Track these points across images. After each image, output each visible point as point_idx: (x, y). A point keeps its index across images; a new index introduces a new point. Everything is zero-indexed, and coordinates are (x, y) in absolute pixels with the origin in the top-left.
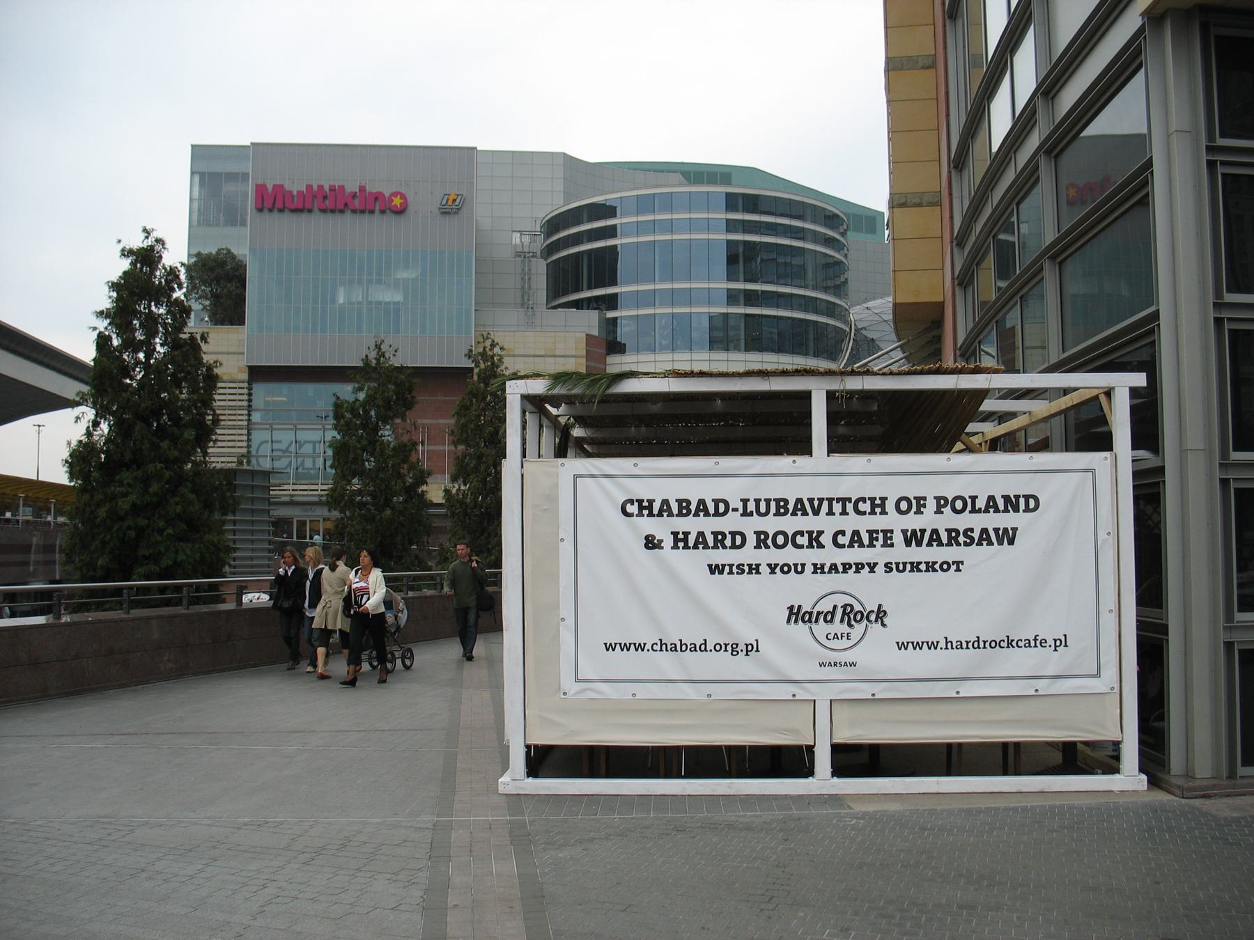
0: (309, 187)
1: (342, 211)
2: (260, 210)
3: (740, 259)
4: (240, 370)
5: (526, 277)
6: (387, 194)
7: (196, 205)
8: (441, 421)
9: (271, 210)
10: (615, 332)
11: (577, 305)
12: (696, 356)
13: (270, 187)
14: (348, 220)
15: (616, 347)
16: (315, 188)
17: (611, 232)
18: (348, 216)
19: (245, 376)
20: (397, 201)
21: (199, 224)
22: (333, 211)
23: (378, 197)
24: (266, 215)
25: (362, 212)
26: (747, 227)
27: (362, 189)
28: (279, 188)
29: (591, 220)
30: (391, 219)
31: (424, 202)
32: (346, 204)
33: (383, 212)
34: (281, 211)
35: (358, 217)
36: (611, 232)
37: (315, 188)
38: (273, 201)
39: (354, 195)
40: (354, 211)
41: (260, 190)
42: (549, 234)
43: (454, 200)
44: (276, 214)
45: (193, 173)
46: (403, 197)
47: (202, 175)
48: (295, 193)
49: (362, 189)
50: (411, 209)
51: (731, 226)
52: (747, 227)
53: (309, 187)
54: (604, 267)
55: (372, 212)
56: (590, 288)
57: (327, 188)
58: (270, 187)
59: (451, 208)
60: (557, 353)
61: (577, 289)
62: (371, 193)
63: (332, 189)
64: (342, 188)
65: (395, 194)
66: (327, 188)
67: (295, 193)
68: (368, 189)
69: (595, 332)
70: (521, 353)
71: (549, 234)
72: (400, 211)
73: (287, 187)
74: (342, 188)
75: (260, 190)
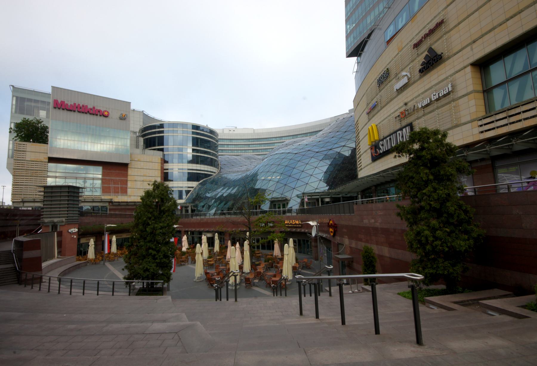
0: (75, 104)
1: (86, 113)
2: (55, 108)
3: (196, 142)
4: (45, 158)
7: (14, 107)
8: (117, 178)
9: (59, 109)
11: (154, 149)
12: (184, 165)
13: (59, 101)
14: (88, 116)
16: (77, 104)
17: (162, 132)
18: (88, 115)
19: (47, 161)
20: (106, 113)
21: (16, 112)
22: (83, 113)
23: (99, 111)
24: (57, 110)
25: (94, 114)
26: (198, 134)
27: (94, 108)
28: (63, 102)
30: (102, 118)
31: (115, 115)
33: (100, 116)
34: (63, 109)
35: (92, 116)
36: (162, 132)
37: (77, 104)
38: (59, 106)
39: (91, 109)
40: (91, 114)
41: (56, 102)
42: (142, 132)
44: (61, 111)
45: (13, 96)
46: (108, 112)
47: (17, 98)
48: (69, 105)
49: (94, 108)
50: (110, 116)
51: (193, 133)
52: (198, 134)
53: (75, 104)
54: (161, 141)
55: (97, 115)
56: (158, 145)
57: (81, 105)
58: (59, 101)
59: (123, 118)
61: (154, 146)
63: (83, 106)
64: (87, 106)
65: (106, 111)
66: (81, 105)
67: (69, 105)
71: (142, 132)
72: (106, 116)
73: (66, 102)
74: (87, 106)
75: (56, 102)
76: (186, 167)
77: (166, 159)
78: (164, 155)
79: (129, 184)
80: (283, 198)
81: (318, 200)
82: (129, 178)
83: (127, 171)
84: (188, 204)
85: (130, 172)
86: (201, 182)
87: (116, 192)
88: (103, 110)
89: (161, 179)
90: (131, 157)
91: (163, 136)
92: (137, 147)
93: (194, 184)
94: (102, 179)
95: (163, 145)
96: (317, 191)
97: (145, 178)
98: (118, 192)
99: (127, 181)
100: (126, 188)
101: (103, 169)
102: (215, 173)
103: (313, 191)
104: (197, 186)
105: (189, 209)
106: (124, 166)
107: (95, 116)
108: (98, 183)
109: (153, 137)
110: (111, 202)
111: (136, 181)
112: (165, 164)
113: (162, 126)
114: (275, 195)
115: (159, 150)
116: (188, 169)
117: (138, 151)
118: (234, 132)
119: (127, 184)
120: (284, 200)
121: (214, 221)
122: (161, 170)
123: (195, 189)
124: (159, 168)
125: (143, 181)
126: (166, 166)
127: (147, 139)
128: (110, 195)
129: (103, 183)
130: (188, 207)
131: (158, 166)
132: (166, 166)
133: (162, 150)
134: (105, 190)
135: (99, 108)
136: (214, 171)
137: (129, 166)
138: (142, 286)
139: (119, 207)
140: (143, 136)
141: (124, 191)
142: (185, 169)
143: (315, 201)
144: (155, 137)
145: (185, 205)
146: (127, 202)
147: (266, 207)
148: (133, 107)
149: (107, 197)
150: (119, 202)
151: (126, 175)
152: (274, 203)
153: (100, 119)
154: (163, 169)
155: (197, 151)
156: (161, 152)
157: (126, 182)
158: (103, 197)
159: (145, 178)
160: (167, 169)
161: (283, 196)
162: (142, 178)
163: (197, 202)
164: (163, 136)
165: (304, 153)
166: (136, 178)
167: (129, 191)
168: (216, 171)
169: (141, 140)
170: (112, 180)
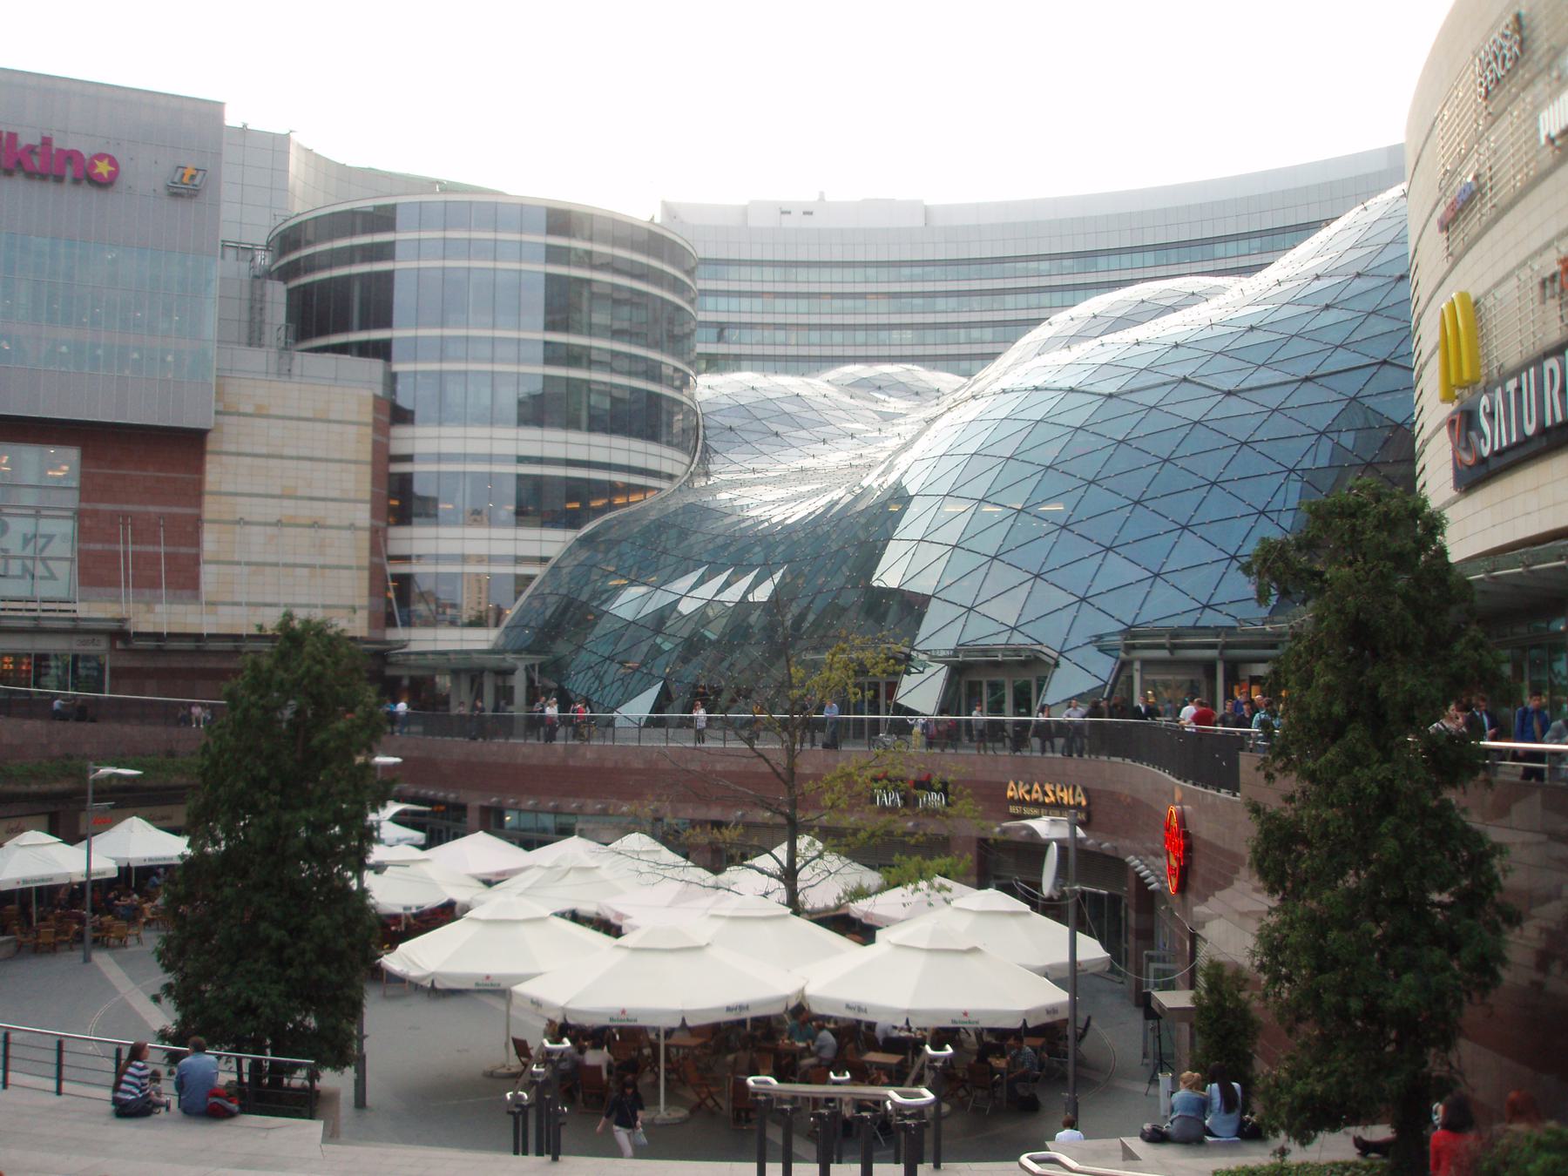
5: (256, 307)
6: (87, 157)
8: (151, 509)
10: (394, 391)
15: (402, 416)
17: (384, 252)
20: (103, 168)
23: (72, 156)
25: (44, 177)
27: (47, 142)
29: (365, 231)
30: (84, 196)
31: (145, 171)
32: (19, 163)
33: (77, 181)
36: (384, 252)
39: (31, 149)
40: (31, 175)
43: (193, 177)
46: (113, 162)
49: (47, 142)
54: (376, 302)
55: (59, 179)
56: (364, 326)
59: (187, 189)
60: (333, 416)
61: (345, 327)
62: (60, 151)
65: (101, 157)
68: (56, 144)
69: (380, 391)
70: (280, 412)
76: (510, 449)
77: (404, 401)
78: (392, 379)
79: (210, 541)
80: (1017, 651)
81: (1209, 668)
82: (210, 508)
83: (199, 469)
84: (510, 659)
85: (216, 473)
86: (587, 528)
87: (146, 580)
88: (87, 151)
89: (375, 514)
90: (220, 395)
91: (389, 276)
92: (254, 338)
93: (553, 542)
94: (80, 515)
95: (387, 323)
96: (1210, 619)
97: (289, 508)
98: (154, 584)
99: (197, 522)
100: (196, 560)
101: (84, 457)
102: (671, 477)
103: (1187, 621)
104: (570, 551)
105: (519, 682)
106: (182, 447)
107: (51, 187)
108: (62, 531)
109: (334, 287)
110: (119, 634)
111: (241, 522)
112: (399, 431)
113: (383, 218)
114: (980, 632)
115: (364, 350)
116: (522, 460)
117: (258, 359)
118: (808, 223)
119: (197, 542)
120: (1025, 664)
121: (638, 764)
122: (375, 464)
123: (556, 568)
124: (366, 453)
125: (279, 523)
126: (404, 439)
127: (306, 290)
128: (117, 601)
129: (84, 533)
130: (511, 672)
131: (357, 443)
132: (404, 439)
133: (382, 351)
134: (95, 571)
135: (70, 145)
136: (667, 467)
137: (210, 446)
138: (234, 1077)
139: (162, 663)
140: (286, 273)
141: (184, 577)
142: (503, 459)
143: (1199, 676)
144: (348, 279)
145: (493, 661)
146: (198, 637)
147: (922, 693)
148: (232, 119)
149: (97, 609)
150: (158, 636)
151: (195, 493)
152: (970, 676)
153: (73, 200)
154: (383, 457)
155: (573, 357)
156: (375, 366)
157: (191, 530)
158: (83, 610)
159: (289, 508)
160: (408, 458)
161: (1018, 639)
162: (273, 510)
163: (562, 648)
164: (389, 276)
165: (1150, 398)
166: (245, 508)
167: (209, 575)
168: (678, 470)
169: (277, 294)
170: (125, 515)
